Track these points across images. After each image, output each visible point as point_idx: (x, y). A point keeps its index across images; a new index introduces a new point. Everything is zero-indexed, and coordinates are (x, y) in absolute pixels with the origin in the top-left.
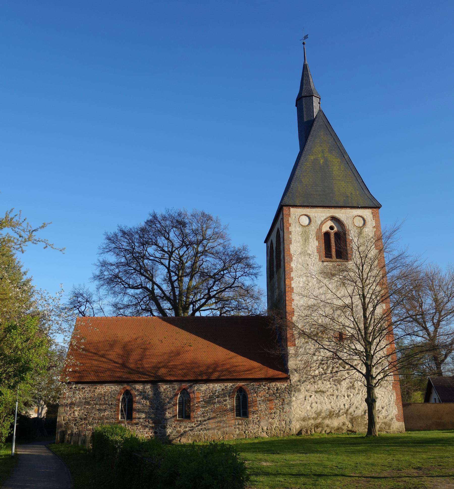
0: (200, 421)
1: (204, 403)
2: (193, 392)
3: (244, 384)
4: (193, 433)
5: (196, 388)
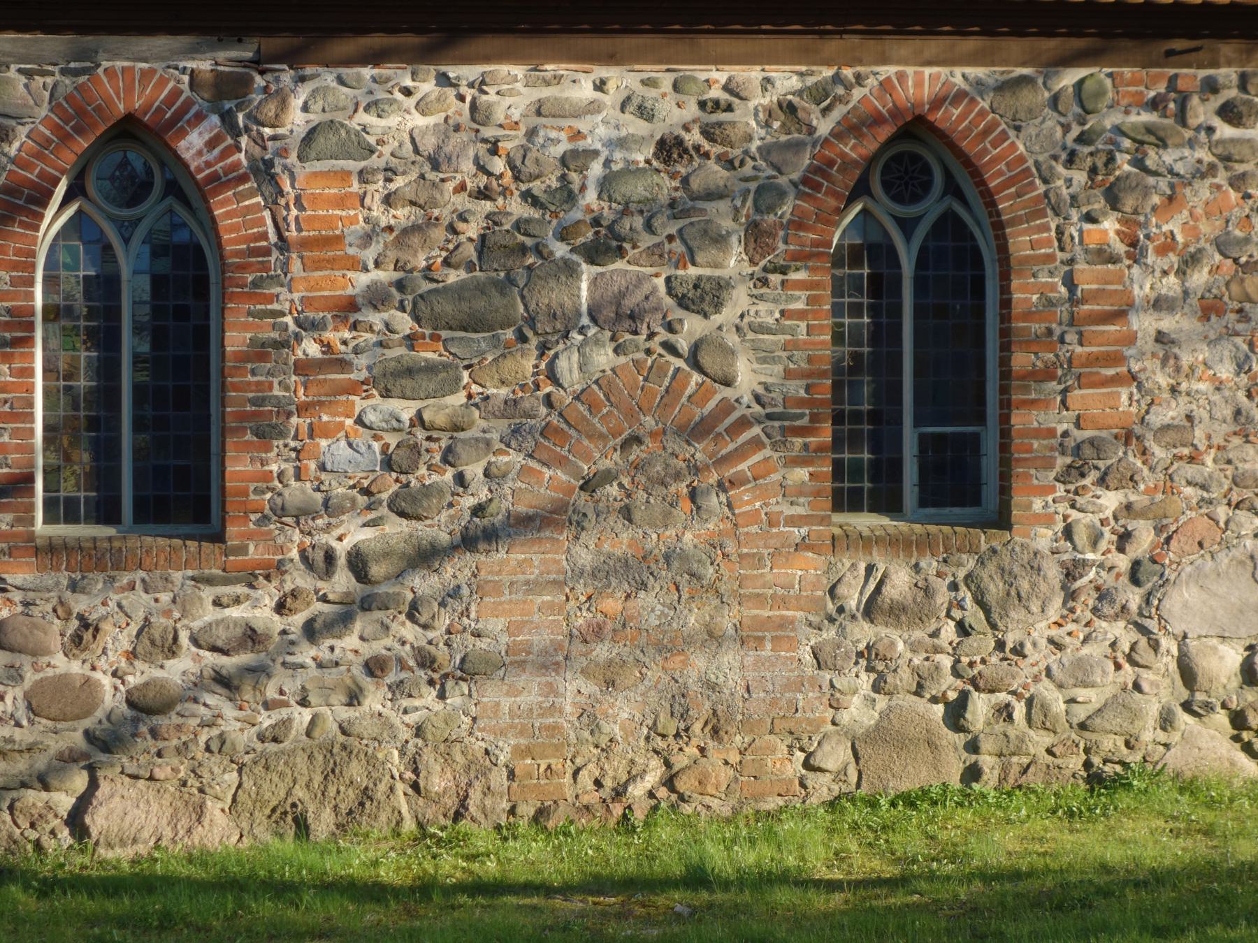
0: (358, 563)
1: (405, 323)
2: (264, 172)
3: (958, 76)
4: (266, 720)
5: (296, 120)
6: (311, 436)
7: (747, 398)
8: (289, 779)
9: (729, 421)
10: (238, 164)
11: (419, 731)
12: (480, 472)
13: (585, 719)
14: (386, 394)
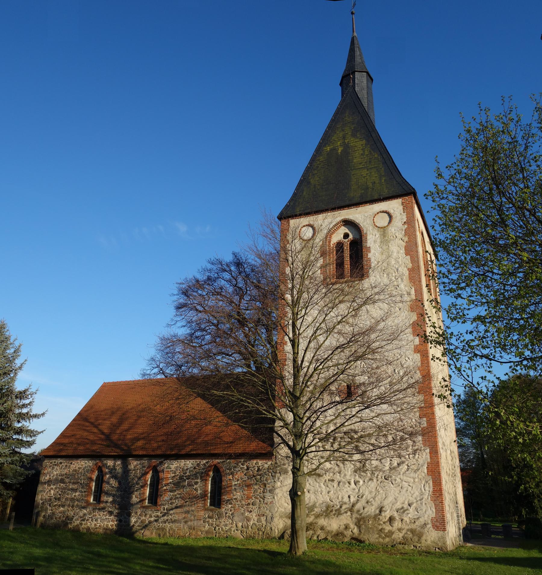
1: (173, 485)
2: (163, 471)
3: (219, 461)
4: (158, 525)
5: (166, 465)
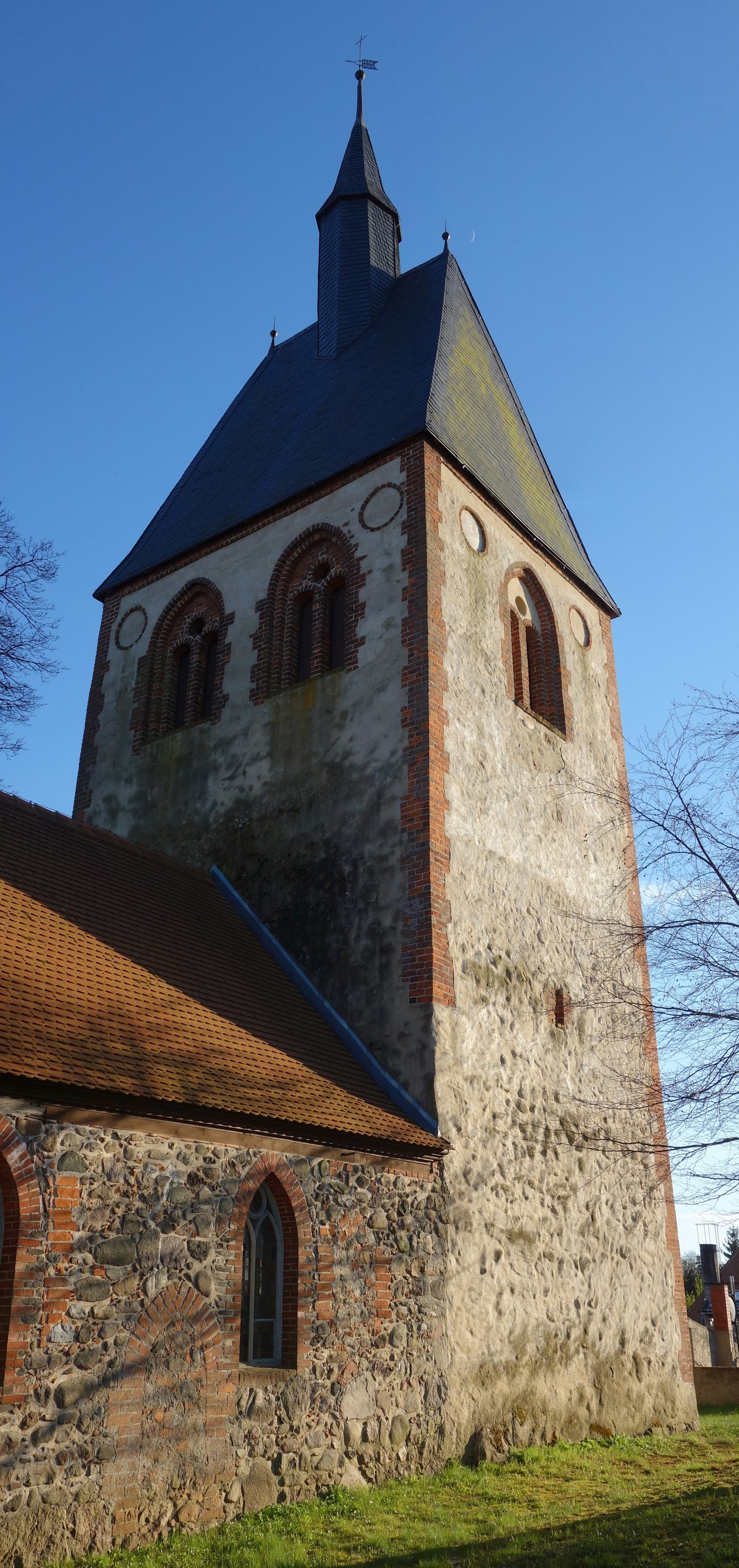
0: (60, 1396)
1: (90, 1258)
2: (43, 1173)
6: (47, 1322)
7: (213, 1304)
8: (16, 1535)
9: (206, 1315)
10: (31, 1169)
11: (77, 1497)
12: (112, 1342)
13: (145, 1483)
14: (80, 1299)
